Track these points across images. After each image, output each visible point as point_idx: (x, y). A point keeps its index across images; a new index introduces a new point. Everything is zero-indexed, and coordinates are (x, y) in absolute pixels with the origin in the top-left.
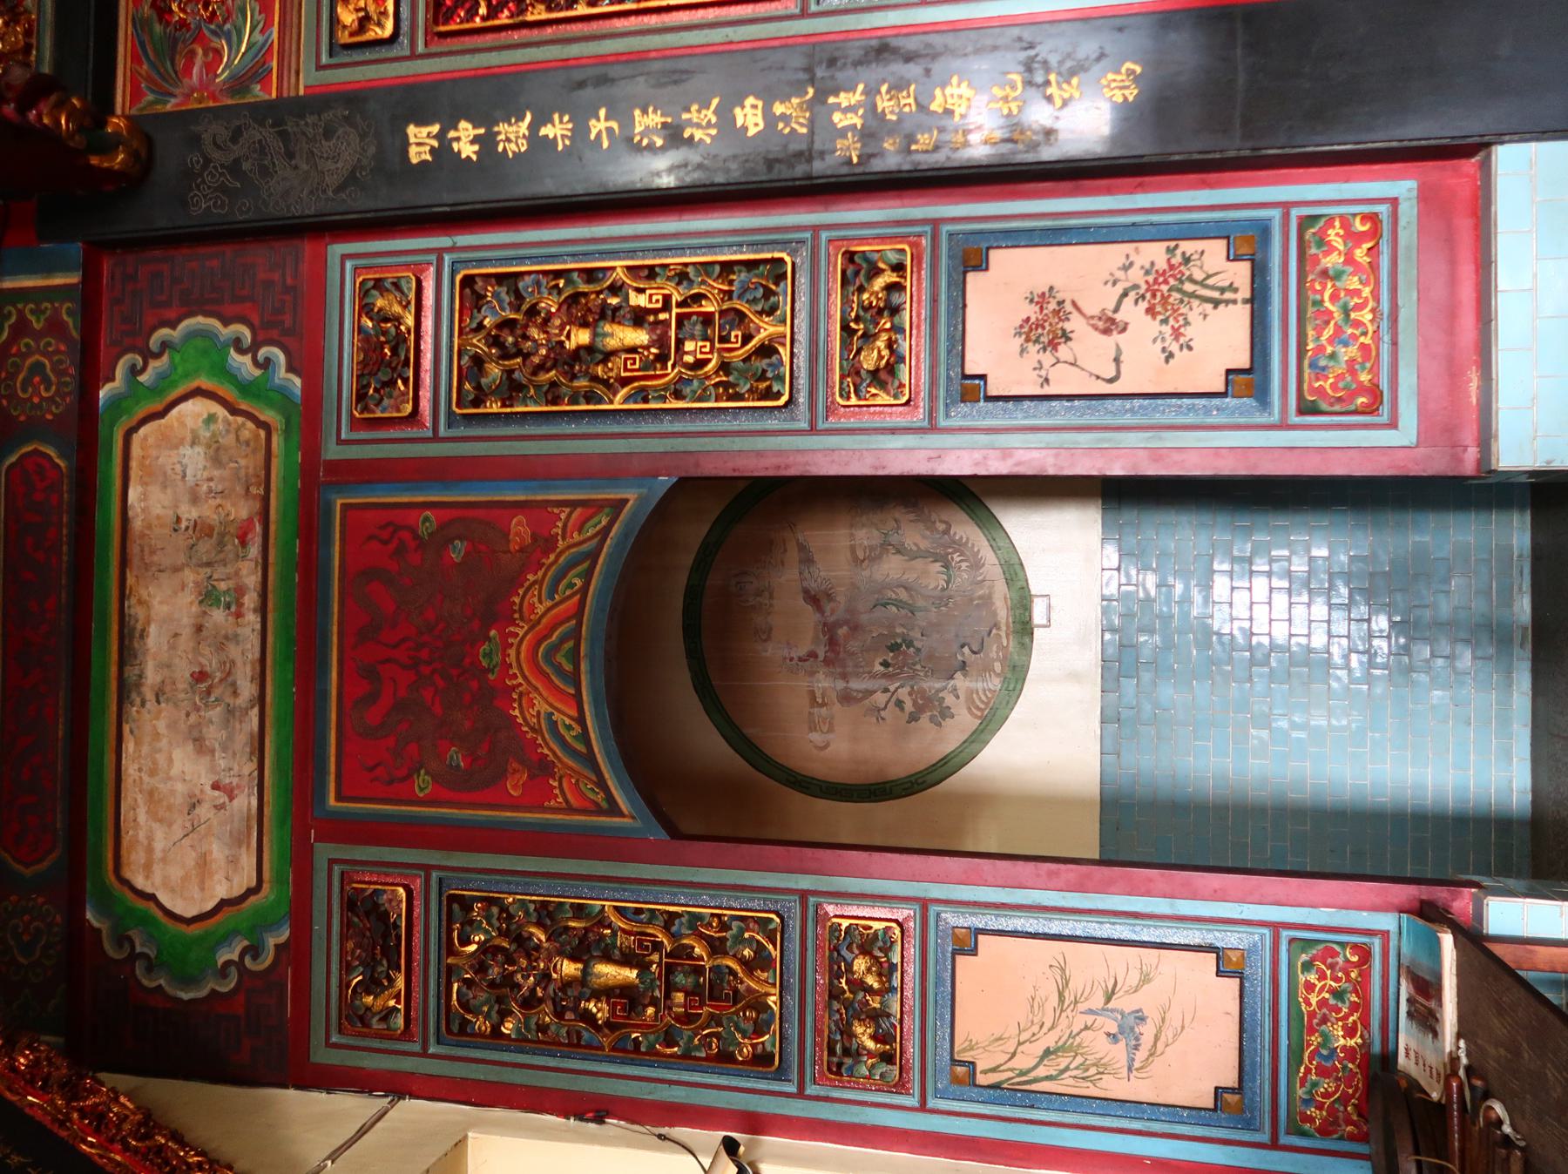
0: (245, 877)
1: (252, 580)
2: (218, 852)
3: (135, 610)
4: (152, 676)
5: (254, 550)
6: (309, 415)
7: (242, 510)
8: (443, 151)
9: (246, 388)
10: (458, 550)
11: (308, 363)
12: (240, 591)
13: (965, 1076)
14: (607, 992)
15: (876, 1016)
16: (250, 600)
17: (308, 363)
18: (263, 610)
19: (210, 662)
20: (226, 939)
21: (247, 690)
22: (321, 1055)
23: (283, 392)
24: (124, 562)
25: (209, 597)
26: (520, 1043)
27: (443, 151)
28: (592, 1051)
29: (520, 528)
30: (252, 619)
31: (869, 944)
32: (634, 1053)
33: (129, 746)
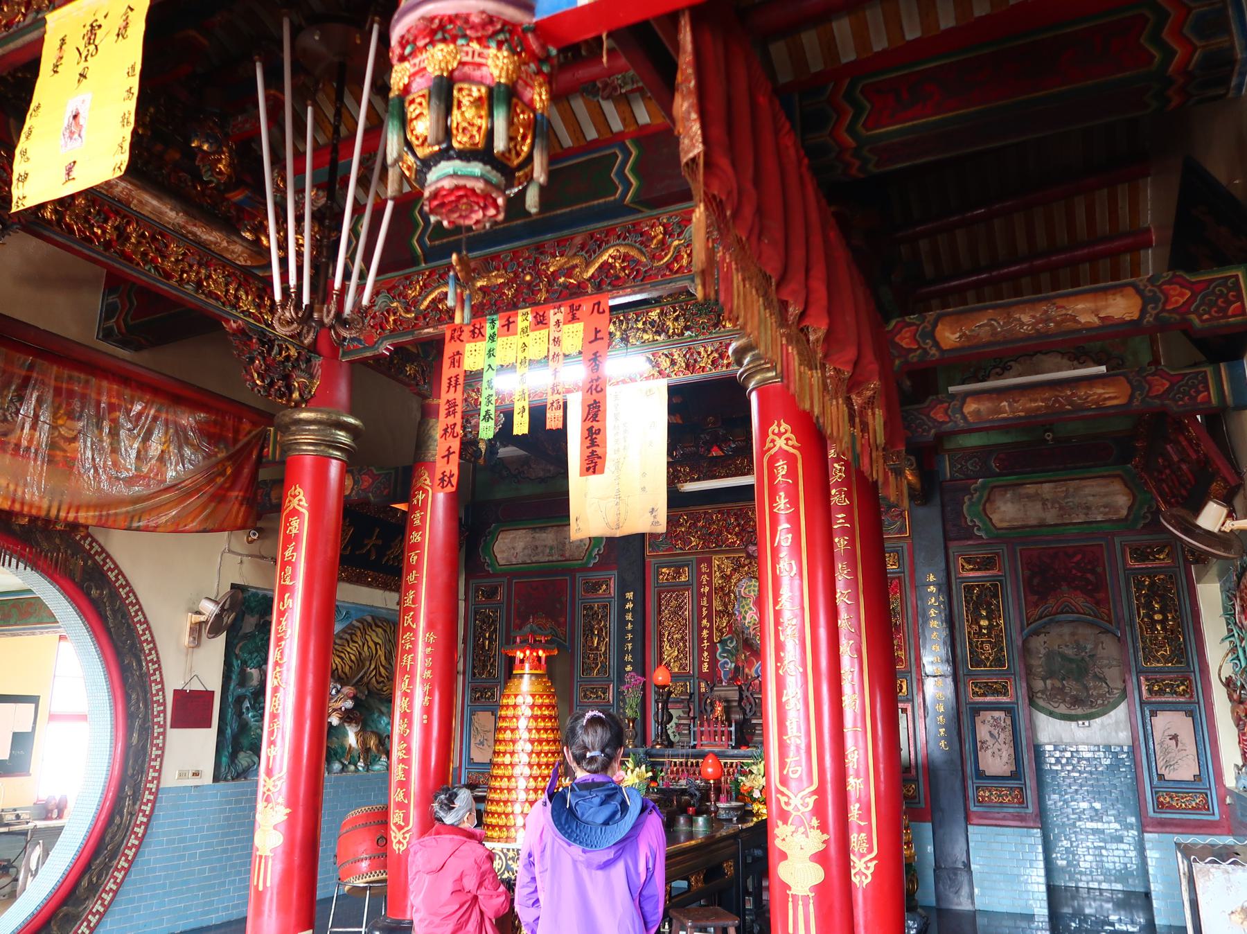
0: (502, 562)
1: (554, 558)
2: (505, 555)
3: (550, 529)
4: (537, 535)
5: (560, 558)
6: (584, 569)
7: (567, 555)
8: (628, 600)
9: (590, 553)
10: (558, 606)
11: (596, 567)
12: (552, 555)
13: (473, 713)
14: (483, 643)
15: (482, 696)
16: (551, 558)
17: (596, 567)
18: (549, 562)
19: (540, 550)
20: (490, 559)
21: (534, 559)
22: (471, 582)
23: (588, 562)
24: (558, 526)
25: (551, 548)
26: (475, 625)
27: (628, 600)
28: (474, 641)
29: (562, 620)
30: (547, 559)
31: (493, 695)
32: (474, 649)
33: (524, 531)
